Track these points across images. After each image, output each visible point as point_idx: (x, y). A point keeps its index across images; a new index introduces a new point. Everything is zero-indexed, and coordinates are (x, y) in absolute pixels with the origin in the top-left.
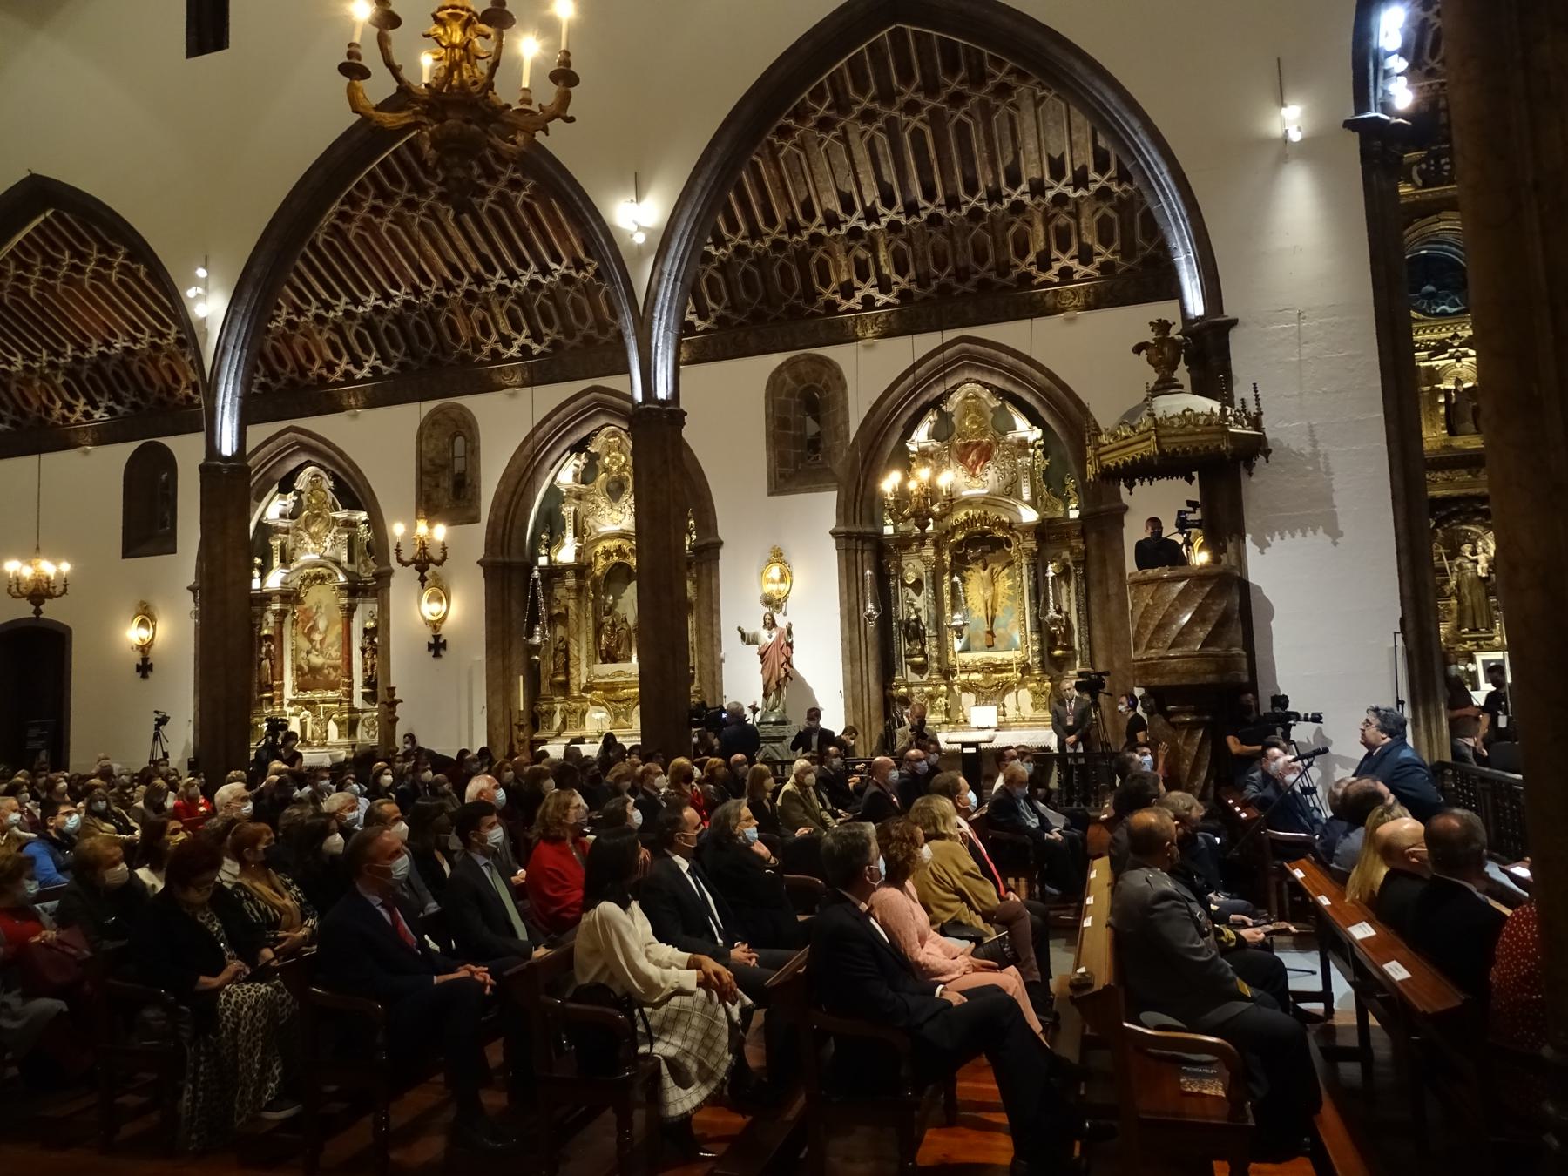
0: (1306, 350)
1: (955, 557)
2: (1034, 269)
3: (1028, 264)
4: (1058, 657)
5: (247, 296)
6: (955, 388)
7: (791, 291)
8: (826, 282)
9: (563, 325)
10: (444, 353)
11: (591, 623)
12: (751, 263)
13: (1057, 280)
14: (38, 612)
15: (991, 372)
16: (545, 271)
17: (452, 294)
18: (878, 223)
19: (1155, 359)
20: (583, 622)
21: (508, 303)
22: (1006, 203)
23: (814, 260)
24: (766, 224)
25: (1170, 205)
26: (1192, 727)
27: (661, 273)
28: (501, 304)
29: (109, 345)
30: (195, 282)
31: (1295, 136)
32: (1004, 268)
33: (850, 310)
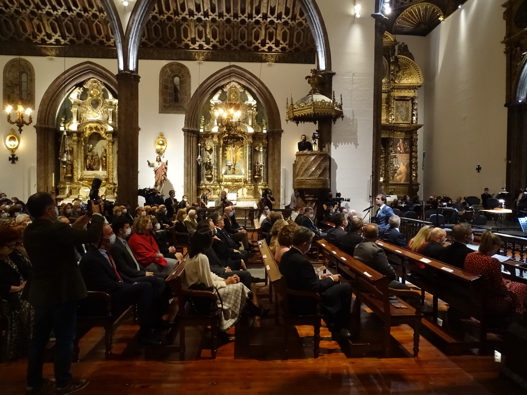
0: (354, 86)
1: (224, 142)
2: (260, 45)
3: (258, 43)
4: (256, 178)
6: (228, 83)
7: (172, 38)
8: (186, 37)
9: (76, 34)
11: (83, 155)
12: (158, 23)
13: (267, 50)
15: (242, 79)
16: (70, 9)
17: (24, 11)
18: (208, 18)
19: (312, 82)
20: (80, 154)
21: (51, 20)
22: (254, 20)
23: (183, 27)
25: (318, 31)
26: (312, 201)
27: (134, 20)
28: (48, 20)
31: (358, 16)
32: (250, 43)
33: (194, 49)
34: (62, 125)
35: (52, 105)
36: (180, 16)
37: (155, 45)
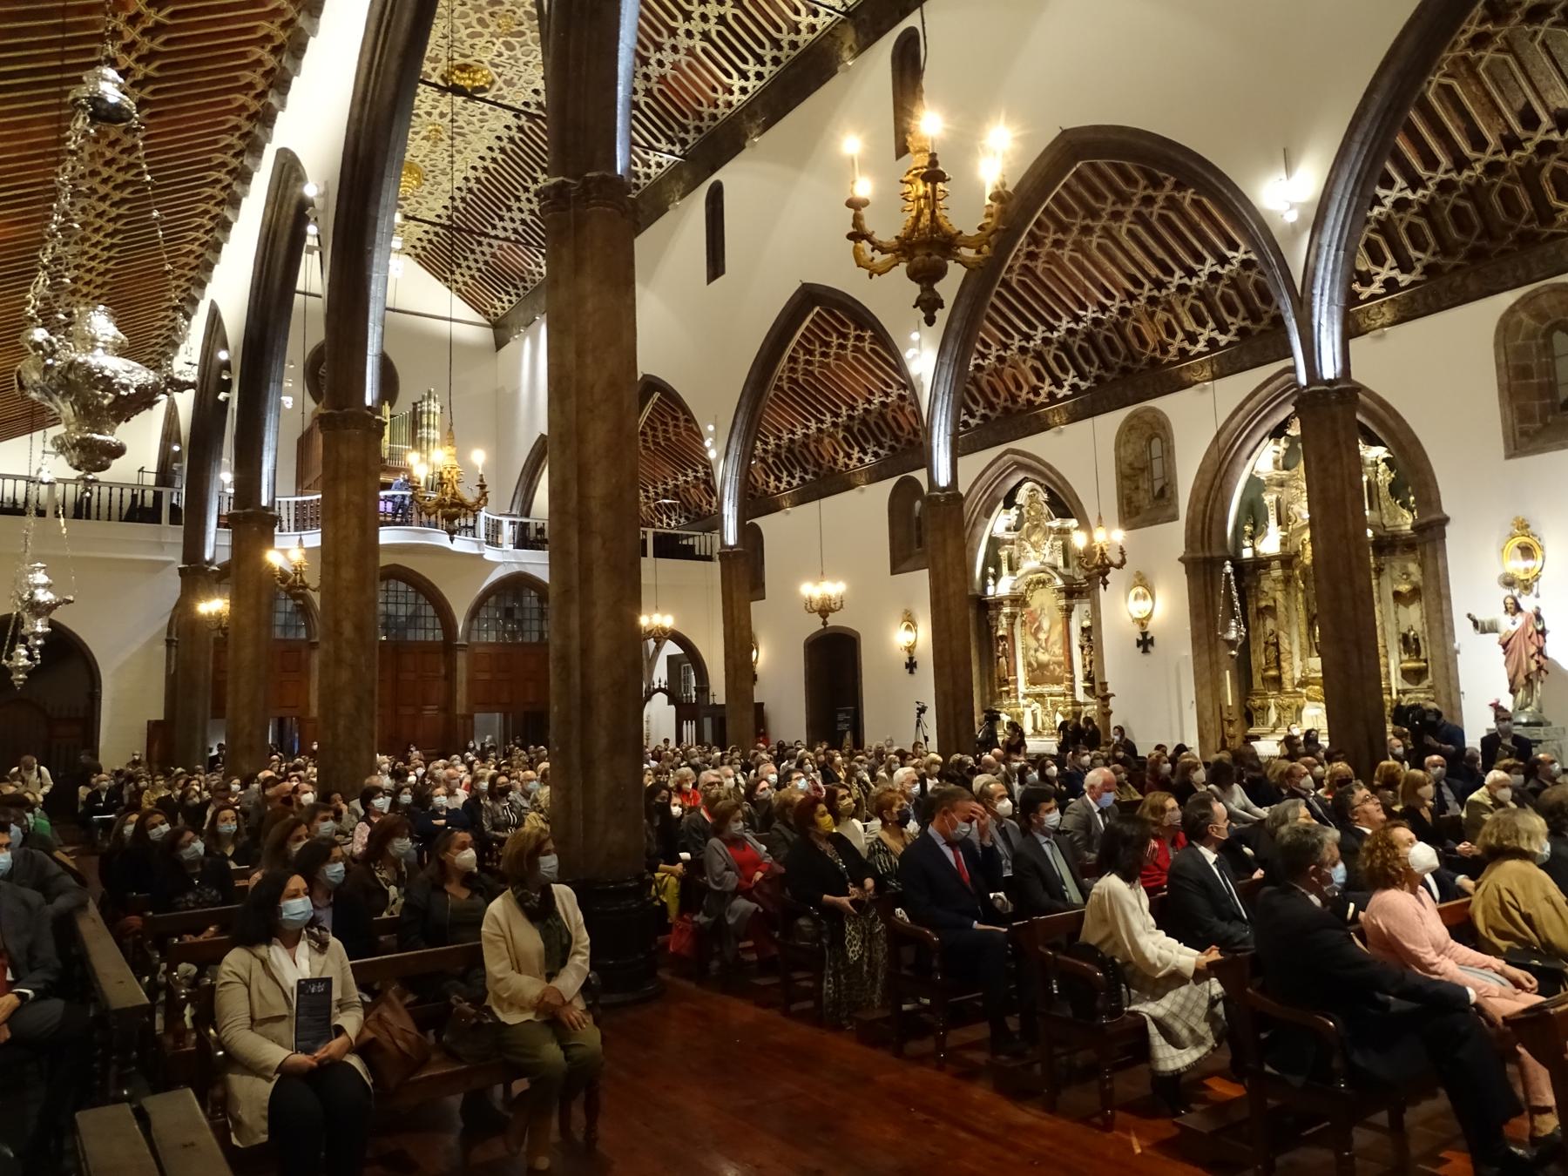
5: (949, 348)
7: (1519, 217)
10: (1135, 360)
11: (1302, 613)
12: (1460, 196)
14: (825, 623)
16: (1223, 260)
20: (1294, 613)
23: (1546, 173)
24: (1474, 149)
27: (1319, 246)
28: (1183, 304)
29: (870, 402)
30: (910, 345)
34: (1247, 543)
35: (1215, 501)
36: (1477, 165)
37: (1465, 258)
